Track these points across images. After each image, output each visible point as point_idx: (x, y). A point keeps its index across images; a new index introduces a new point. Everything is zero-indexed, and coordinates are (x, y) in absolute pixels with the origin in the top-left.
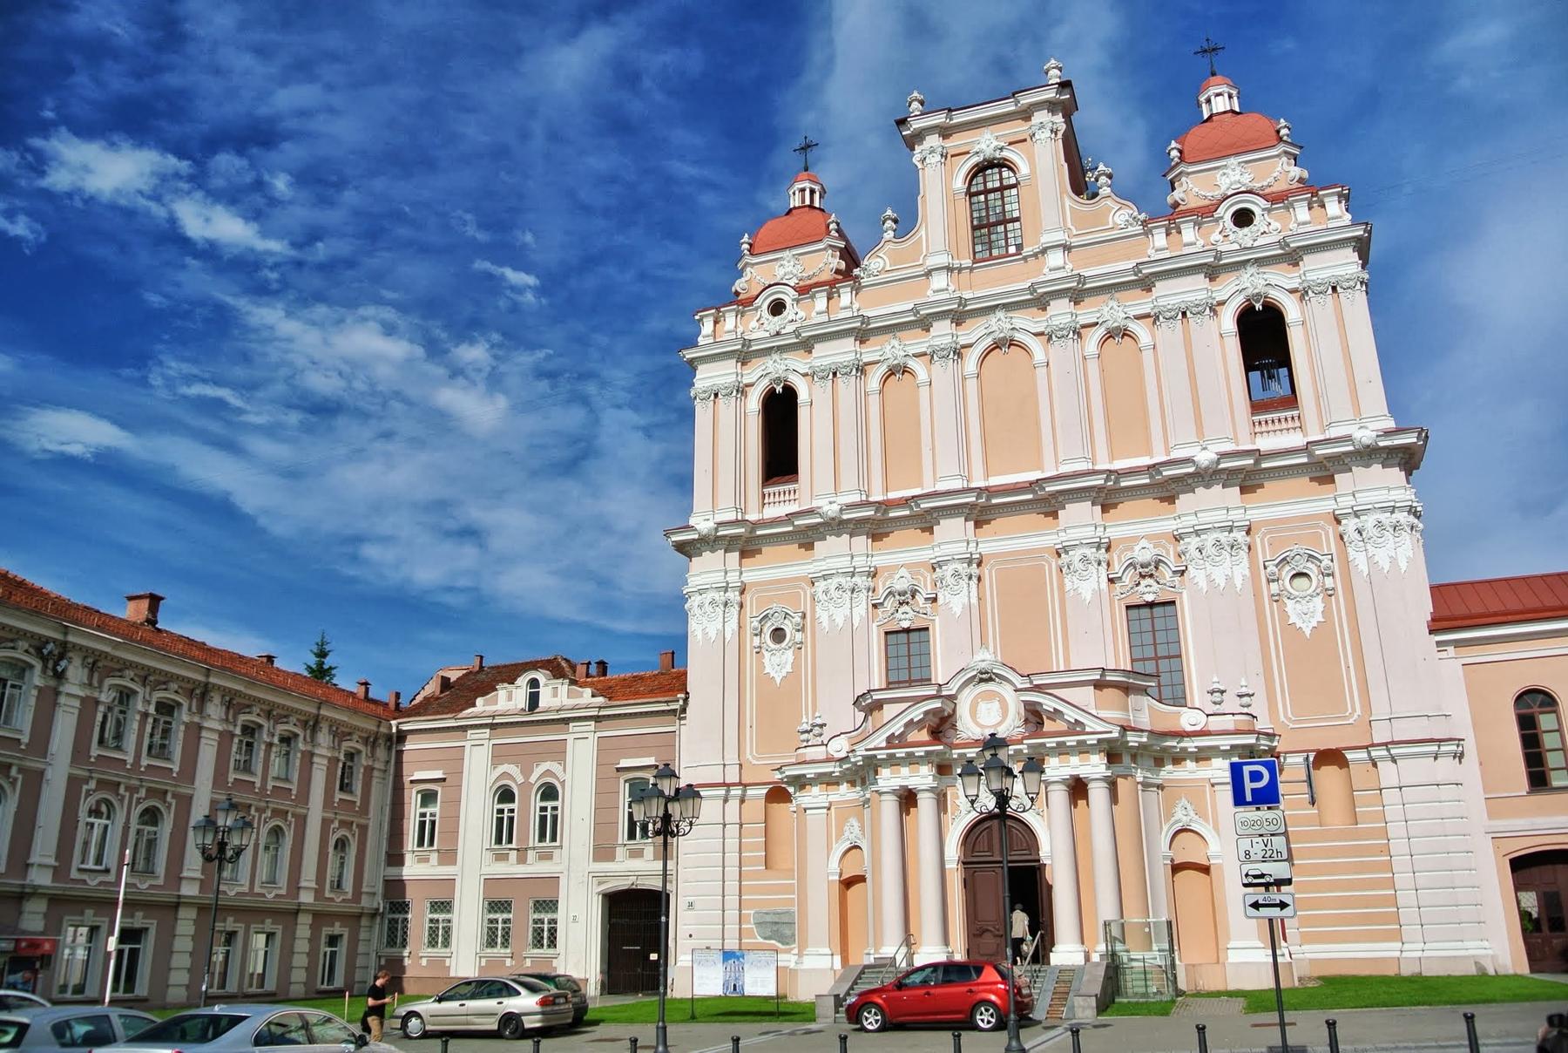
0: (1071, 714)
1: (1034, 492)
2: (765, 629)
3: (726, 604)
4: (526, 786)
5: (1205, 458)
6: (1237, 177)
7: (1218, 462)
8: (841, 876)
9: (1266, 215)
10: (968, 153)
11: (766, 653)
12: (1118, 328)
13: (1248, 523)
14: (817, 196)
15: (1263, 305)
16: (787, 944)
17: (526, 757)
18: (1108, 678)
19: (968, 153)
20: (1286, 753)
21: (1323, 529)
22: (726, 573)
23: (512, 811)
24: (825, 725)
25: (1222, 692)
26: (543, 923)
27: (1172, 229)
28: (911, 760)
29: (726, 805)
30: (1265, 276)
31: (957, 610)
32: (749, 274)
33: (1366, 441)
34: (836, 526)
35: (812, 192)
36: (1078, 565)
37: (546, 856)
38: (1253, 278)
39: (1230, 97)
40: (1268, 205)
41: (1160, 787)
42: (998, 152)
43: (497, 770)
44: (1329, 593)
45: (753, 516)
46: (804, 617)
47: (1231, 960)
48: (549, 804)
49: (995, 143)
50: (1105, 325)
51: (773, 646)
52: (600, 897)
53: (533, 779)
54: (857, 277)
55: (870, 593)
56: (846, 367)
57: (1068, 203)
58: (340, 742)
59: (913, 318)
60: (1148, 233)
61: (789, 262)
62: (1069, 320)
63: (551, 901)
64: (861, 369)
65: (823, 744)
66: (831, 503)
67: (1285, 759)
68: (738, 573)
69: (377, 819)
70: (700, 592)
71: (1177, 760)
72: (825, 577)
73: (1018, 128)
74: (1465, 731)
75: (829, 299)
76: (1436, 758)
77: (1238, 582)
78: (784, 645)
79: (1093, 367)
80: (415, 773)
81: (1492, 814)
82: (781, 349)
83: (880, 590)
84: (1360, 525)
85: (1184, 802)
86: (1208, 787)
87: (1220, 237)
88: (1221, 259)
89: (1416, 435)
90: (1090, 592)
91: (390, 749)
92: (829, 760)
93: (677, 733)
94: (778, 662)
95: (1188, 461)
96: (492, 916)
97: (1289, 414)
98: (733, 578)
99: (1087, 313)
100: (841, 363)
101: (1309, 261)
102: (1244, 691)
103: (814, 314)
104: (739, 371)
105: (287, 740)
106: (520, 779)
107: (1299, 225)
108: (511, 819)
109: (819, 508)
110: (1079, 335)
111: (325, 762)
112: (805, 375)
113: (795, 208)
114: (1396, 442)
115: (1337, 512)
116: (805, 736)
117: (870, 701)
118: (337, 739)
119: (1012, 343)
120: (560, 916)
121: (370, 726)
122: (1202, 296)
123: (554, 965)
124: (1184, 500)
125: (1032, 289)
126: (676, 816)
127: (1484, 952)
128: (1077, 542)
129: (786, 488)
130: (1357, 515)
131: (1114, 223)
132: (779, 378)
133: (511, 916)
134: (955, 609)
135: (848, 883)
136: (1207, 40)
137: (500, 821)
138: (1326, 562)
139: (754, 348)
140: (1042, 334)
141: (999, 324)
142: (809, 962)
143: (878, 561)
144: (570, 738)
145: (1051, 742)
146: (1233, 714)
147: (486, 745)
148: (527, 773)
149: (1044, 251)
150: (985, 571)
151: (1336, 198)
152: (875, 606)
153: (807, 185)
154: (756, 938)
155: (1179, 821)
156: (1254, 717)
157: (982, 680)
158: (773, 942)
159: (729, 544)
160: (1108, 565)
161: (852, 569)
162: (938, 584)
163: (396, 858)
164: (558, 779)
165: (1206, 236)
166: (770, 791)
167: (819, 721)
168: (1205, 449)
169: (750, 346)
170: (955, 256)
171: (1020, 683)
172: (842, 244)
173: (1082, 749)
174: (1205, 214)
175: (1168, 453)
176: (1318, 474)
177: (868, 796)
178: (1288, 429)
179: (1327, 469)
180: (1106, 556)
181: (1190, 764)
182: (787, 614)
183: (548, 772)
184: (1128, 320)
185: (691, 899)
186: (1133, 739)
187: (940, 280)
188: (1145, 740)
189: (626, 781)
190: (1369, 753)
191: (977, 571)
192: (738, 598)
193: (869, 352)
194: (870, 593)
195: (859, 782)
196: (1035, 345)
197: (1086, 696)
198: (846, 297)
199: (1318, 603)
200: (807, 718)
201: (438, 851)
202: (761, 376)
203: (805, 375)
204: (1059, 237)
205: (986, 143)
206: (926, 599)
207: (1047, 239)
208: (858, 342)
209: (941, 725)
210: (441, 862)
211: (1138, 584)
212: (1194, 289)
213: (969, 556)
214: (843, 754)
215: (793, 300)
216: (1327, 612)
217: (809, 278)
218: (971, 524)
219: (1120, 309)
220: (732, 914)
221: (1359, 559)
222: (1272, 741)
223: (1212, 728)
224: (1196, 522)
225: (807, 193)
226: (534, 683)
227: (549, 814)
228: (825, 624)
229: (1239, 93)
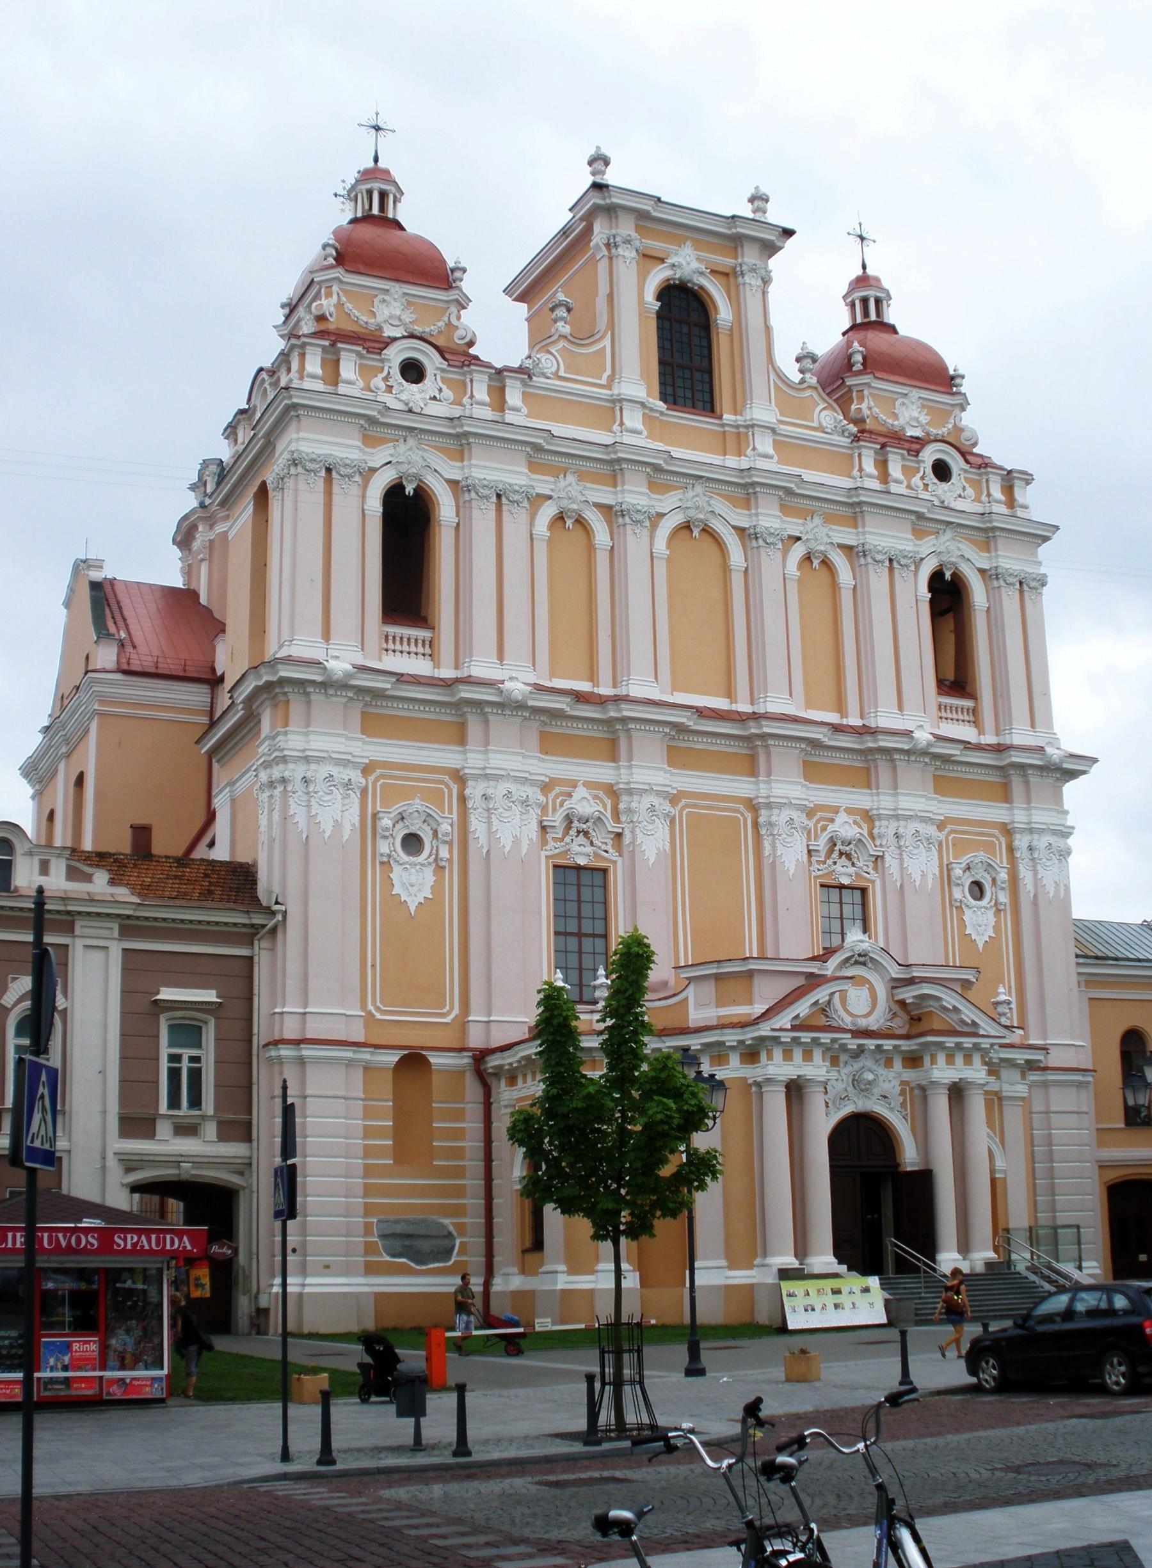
0: (969, 1014)
9: (962, 476)
15: (954, 575)
16: (424, 1263)
19: (662, 260)
30: (960, 545)
38: (948, 543)
40: (967, 467)
49: (695, 265)
51: (405, 857)
66: (511, 679)
73: (725, 261)
81: (1100, 1144)
93: (256, 959)
95: (908, 734)
100: (511, 485)
109: (502, 682)
112: (448, 481)
119: (707, 531)
131: (820, 423)
136: (860, 224)
145: (950, 1041)
153: (376, 186)
154: (379, 1254)
157: (856, 962)
166: (403, 1060)
192: (363, 781)
203: (448, 481)
216: (997, 928)
219: (825, 530)
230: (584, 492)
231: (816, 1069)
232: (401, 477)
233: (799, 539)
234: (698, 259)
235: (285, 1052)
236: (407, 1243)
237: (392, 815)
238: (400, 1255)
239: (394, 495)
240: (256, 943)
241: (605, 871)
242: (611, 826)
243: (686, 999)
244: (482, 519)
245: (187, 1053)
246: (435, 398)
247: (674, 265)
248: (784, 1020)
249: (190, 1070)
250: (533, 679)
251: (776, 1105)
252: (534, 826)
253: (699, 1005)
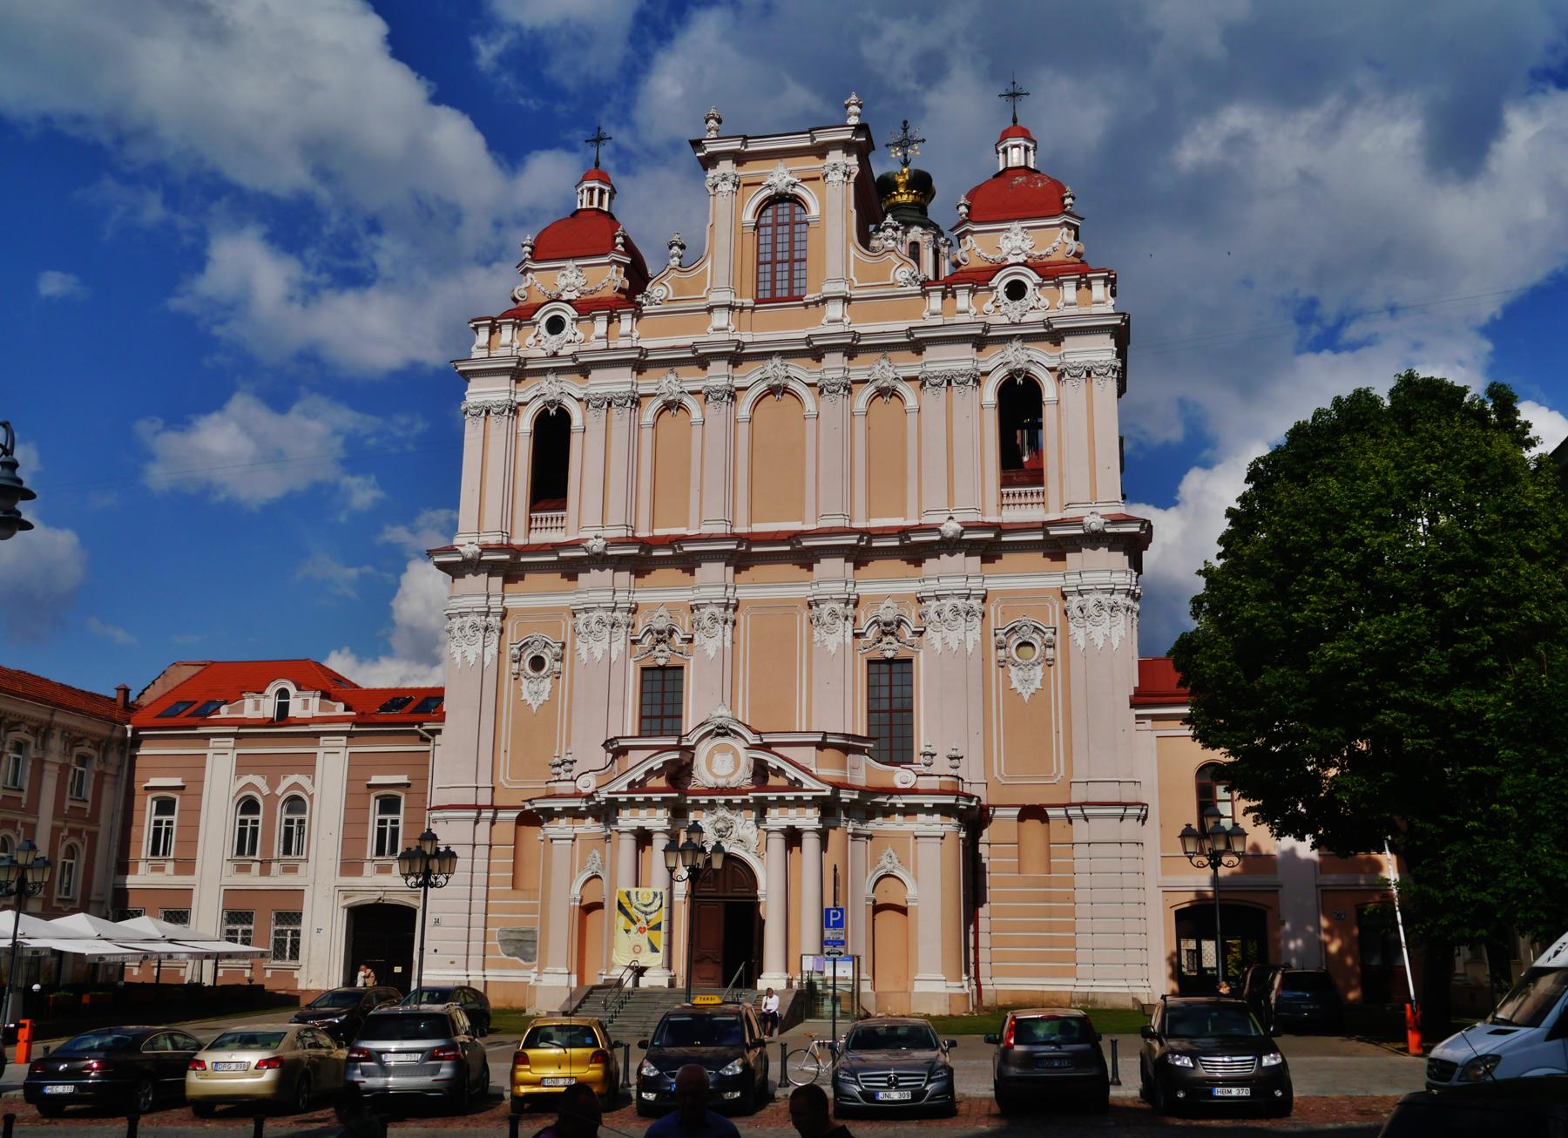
0: (792, 773)
1: (791, 545)
2: (525, 656)
3: (486, 629)
4: (271, 799)
5: (951, 528)
6: (1019, 243)
7: (962, 533)
8: (581, 901)
10: (760, 184)
11: (525, 682)
12: (887, 388)
13: (984, 592)
14: (606, 197)
16: (530, 961)
17: (273, 768)
18: (828, 740)
19: (760, 184)
20: (994, 806)
21: (1051, 603)
22: (488, 597)
23: (256, 822)
24: (575, 761)
25: (933, 755)
26: (286, 935)
27: (948, 291)
28: (648, 804)
29: (477, 826)
31: (711, 652)
32: (529, 280)
33: (1094, 527)
34: (599, 561)
35: (602, 192)
36: (826, 618)
37: (292, 869)
38: (1017, 353)
39: (1027, 149)
41: (870, 837)
42: (790, 187)
43: (241, 780)
44: (1050, 663)
45: (519, 540)
46: (564, 646)
47: (916, 990)
48: (296, 817)
49: (789, 178)
50: (875, 384)
51: (532, 674)
52: (346, 911)
53: (279, 791)
54: (640, 304)
55: (630, 629)
56: (621, 398)
57: (853, 252)
58: (73, 746)
59: (691, 355)
60: (925, 294)
61: (571, 272)
62: (841, 375)
63: (295, 914)
64: (636, 401)
65: (571, 780)
66: (596, 537)
67: (994, 811)
68: (500, 599)
69: (106, 826)
70: (461, 615)
71: (888, 812)
72: (586, 610)
74: (1149, 795)
75: (610, 322)
76: (1122, 820)
77: (970, 647)
78: (542, 673)
79: (860, 423)
80: (151, 780)
81: (1165, 872)
82: (558, 371)
83: (640, 626)
84: (1082, 604)
85: (890, 850)
86: (912, 838)
87: (992, 308)
88: (988, 331)
89: (1139, 525)
90: (835, 645)
91: (122, 753)
92: (577, 795)
93: (431, 752)
94: (536, 691)
95: (934, 529)
96: (231, 927)
97: (1035, 489)
98: (495, 602)
99: (861, 368)
101: (1069, 343)
102: (954, 753)
103: (592, 338)
104: (513, 389)
105: (19, 747)
106: (266, 791)
107: (1065, 305)
108: (254, 831)
109: (587, 540)
110: (851, 391)
111: (56, 768)
112: (579, 400)
113: (582, 210)
114: (1122, 530)
115: (1064, 589)
116: (557, 770)
117: (616, 746)
118: (68, 745)
120: (305, 927)
121: (101, 729)
122: (966, 366)
123: (295, 976)
124: (930, 565)
125: (808, 340)
126: (436, 870)
127: (1143, 990)
128: (827, 597)
129: (554, 514)
130: (1080, 593)
132: (553, 401)
133: (252, 927)
134: (709, 651)
135: (588, 909)
136: (1014, 83)
137: (242, 832)
138: (1049, 635)
139: (528, 367)
140: (814, 385)
141: (774, 370)
142: (548, 981)
143: (641, 597)
144: (320, 752)
145: (772, 796)
146: (940, 776)
147: (230, 754)
148: (273, 784)
149: (825, 301)
150: (741, 617)
151: (1102, 282)
152: (634, 642)
153: (596, 184)
155: (884, 867)
156: (958, 778)
157: (718, 734)
159: (493, 569)
160: (855, 620)
161: (613, 605)
162: (695, 625)
163: (124, 867)
164: (307, 793)
165: (979, 305)
167: (569, 758)
168: (951, 518)
169: (526, 365)
170: (739, 295)
171: (753, 739)
172: (627, 260)
173: (799, 803)
174: (979, 279)
175: (920, 518)
176: (1049, 551)
177: (609, 832)
178: (1032, 504)
179: (1060, 547)
180: (854, 612)
181: (898, 818)
182: (547, 643)
183: (296, 785)
184: (897, 381)
185: (437, 916)
186: (845, 796)
187: (720, 319)
188: (856, 797)
189: (376, 798)
190: (1066, 811)
191: (733, 617)
192: (500, 624)
193: (647, 383)
194: (630, 629)
195: (603, 818)
196: (807, 395)
197: (806, 756)
198: (626, 324)
199: (1038, 672)
200: (560, 751)
201: (174, 860)
202: (536, 394)
203: (579, 400)
204: (842, 288)
205: (780, 175)
206: (683, 639)
207: (829, 289)
208: (635, 373)
209: (679, 773)
210: (177, 872)
211: (879, 642)
212: (960, 358)
213: (726, 601)
214: (589, 790)
215: (573, 320)
217: (591, 292)
218: (731, 570)
219: (891, 369)
220: (477, 932)
221: (1079, 636)
222: (971, 802)
223: (920, 787)
224: (937, 587)
225: (596, 193)
226: (283, 693)
227: (295, 826)
228: (584, 655)
229: (1036, 146)
230: (683, 385)
231: (657, 820)
233: (867, 381)
234: (791, 172)
235: (436, 815)
238: (513, 955)
239: (542, 420)
241: (681, 668)
245: (389, 817)
247: (769, 186)
249: (391, 828)
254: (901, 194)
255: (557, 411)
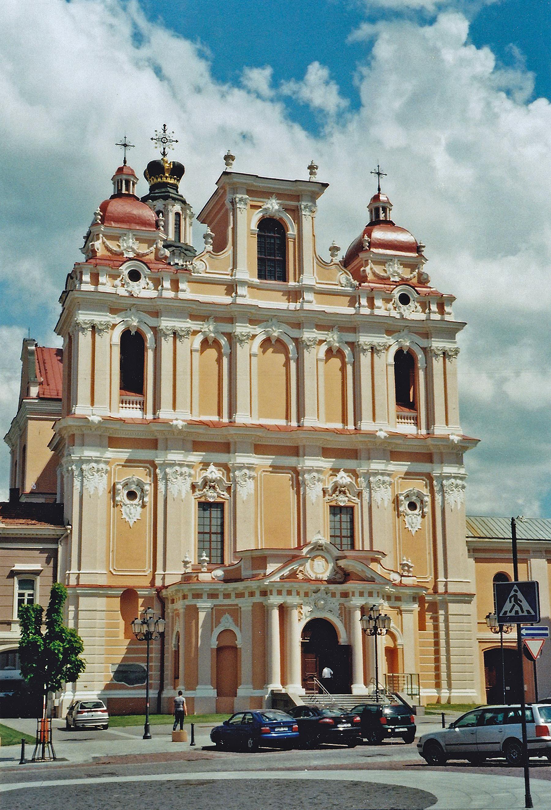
66: (177, 419)
109: (172, 421)
134: (242, 495)
157: (318, 550)
158: (123, 683)
211: (337, 496)
232: (129, 327)
236: (124, 675)
237: (122, 483)
240: (59, 542)
242: (226, 483)
243: (240, 566)
244: (167, 345)
245: (27, 592)
246: (144, 288)
248: (277, 578)
250: (189, 417)
251: (275, 614)
252: (189, 486)
253: (246, 569)
254: (167, 177)
255: (135, 332)
